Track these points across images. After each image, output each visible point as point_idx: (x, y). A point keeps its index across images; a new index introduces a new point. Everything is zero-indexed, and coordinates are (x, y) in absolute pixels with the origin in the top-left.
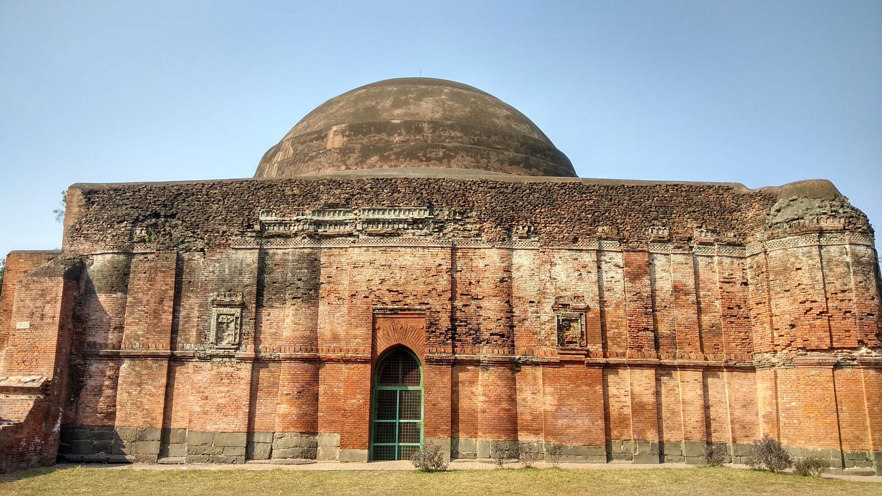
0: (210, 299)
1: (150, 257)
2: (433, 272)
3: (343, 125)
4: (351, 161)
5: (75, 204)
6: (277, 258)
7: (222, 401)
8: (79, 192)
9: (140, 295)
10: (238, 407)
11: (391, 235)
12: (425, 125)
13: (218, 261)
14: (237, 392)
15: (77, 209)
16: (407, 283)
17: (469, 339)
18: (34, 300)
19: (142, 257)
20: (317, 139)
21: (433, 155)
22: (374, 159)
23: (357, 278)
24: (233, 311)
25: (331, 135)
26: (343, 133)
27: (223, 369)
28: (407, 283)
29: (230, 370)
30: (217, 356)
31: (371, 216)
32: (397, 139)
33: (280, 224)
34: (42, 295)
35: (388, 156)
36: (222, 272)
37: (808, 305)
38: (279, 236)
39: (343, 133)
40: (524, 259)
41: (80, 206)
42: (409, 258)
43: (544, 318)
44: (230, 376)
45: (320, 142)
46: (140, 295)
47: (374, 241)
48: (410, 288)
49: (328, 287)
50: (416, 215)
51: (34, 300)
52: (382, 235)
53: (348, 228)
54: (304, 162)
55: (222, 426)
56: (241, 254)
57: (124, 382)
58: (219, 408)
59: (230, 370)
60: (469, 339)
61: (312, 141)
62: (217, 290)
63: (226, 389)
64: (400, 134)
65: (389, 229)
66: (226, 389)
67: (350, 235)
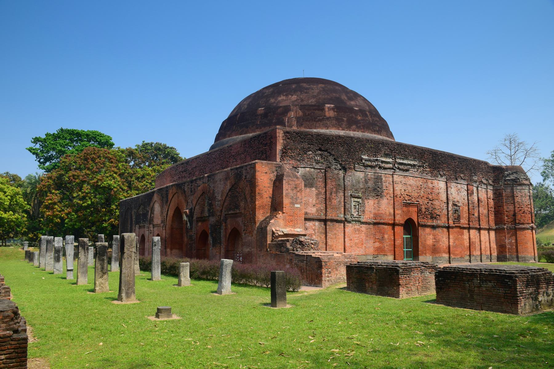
0: (349, 194)
1: (323, 171)
2: (419, 188)
3: (332, 105)
4: (344, 126)
5: (281, 138)
6: (369, 176)
7: (357, 241)
8: (282, 132)
9: (321, 190)
10: (362, 244)
11: (407, 170)
12: (367, 113)
13: (350, 176)
14: (362, 237)
15: (282, 141)
16: (412, 192)
17: (429, 216)
18: (293, 190)
19: (319, 171)
20: (319, 110)
21: (375, 129)
22: (354, 127)
23: (397, 188)
24: (359, 200)
25: (327, 110)
26: (333, 109)
27: (356, 227)
28: (412, 192)
29: (358, 227)
30: (353, 221)
31: (401, 161)
32: (359, 118)
33: (370, 160)
34: (296, 188)
35: (360, 126)
36: (352, 181)
37: (520, 209)
38: (370, 166)
39: (333, 109)
40: (440, 184)
41: (283, 140)
42: (411, 181)
43: (450, 209)
44: (359, 230)
45: (320, 112)
46: (321, 190)
47: (401, 173)
48: (413, 194)
49: (386, 191)
50: (412, 163)
51: (293, 190)
52: (404, 170)
53: (391, 166)
54: (315, 121)
55: (357, 252)
56: (358, 174)
57: (318, 232)
58: (356, 244)
59: (358, 227)
60: (429, 216)
61: (315, 110)
62: (351, 190)
63: (358, 236)
64: (360, 116)
65: (406, 168)
66: (358, 236)
67: (393, 169)
